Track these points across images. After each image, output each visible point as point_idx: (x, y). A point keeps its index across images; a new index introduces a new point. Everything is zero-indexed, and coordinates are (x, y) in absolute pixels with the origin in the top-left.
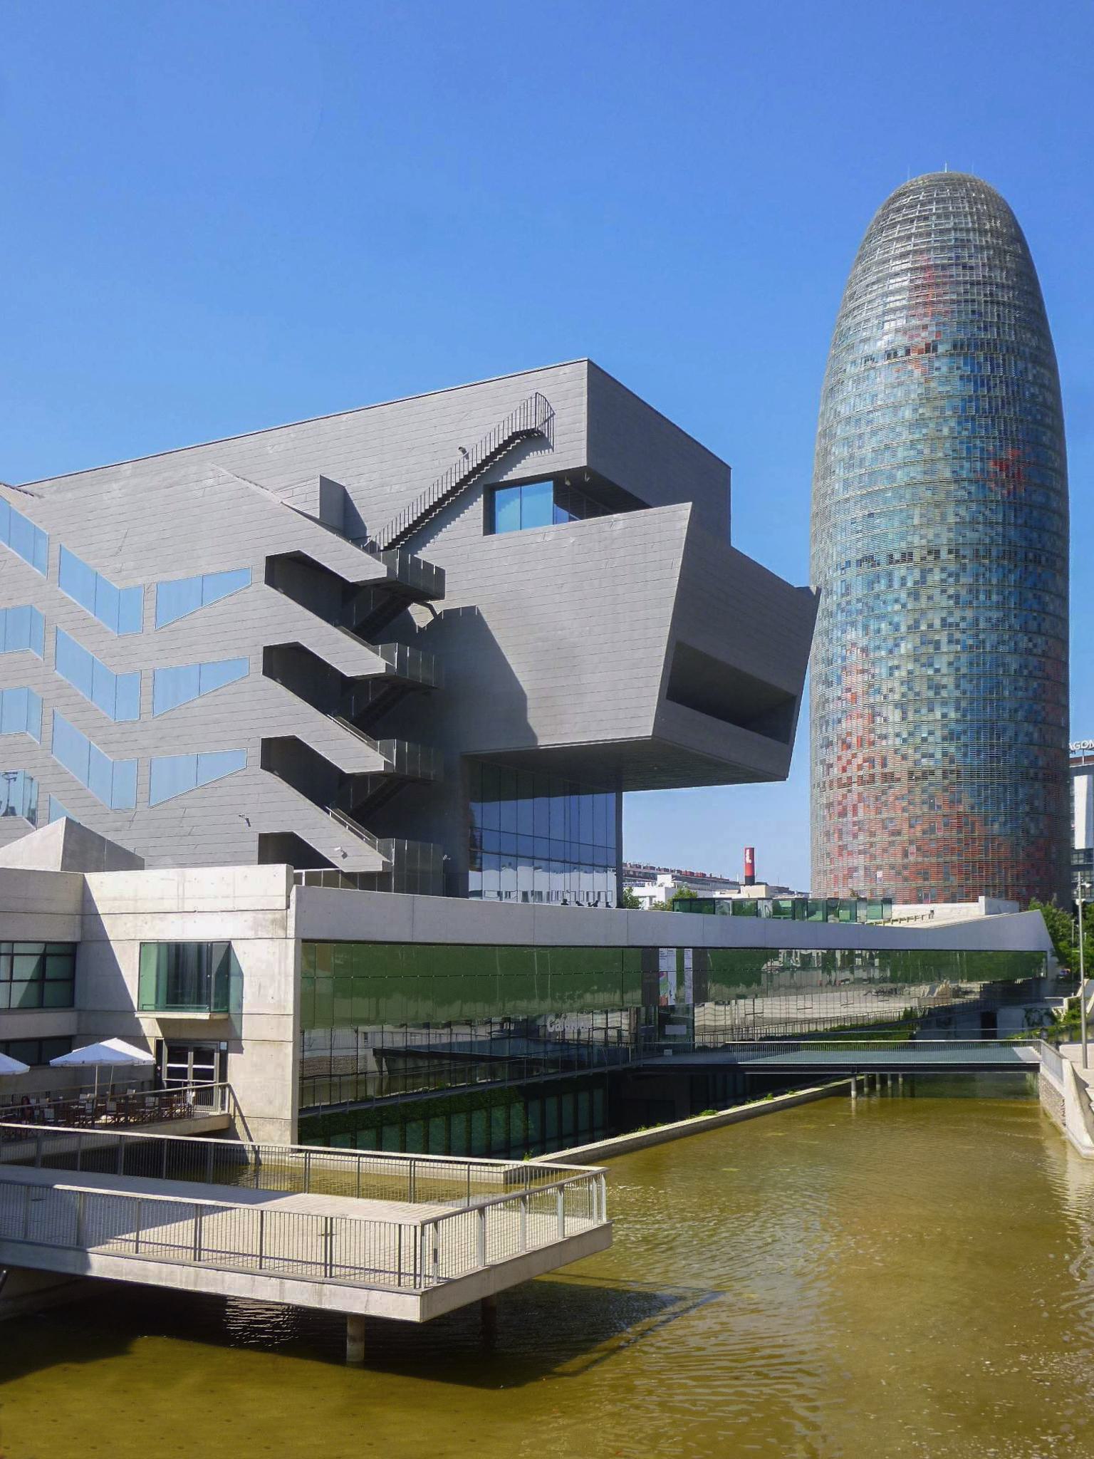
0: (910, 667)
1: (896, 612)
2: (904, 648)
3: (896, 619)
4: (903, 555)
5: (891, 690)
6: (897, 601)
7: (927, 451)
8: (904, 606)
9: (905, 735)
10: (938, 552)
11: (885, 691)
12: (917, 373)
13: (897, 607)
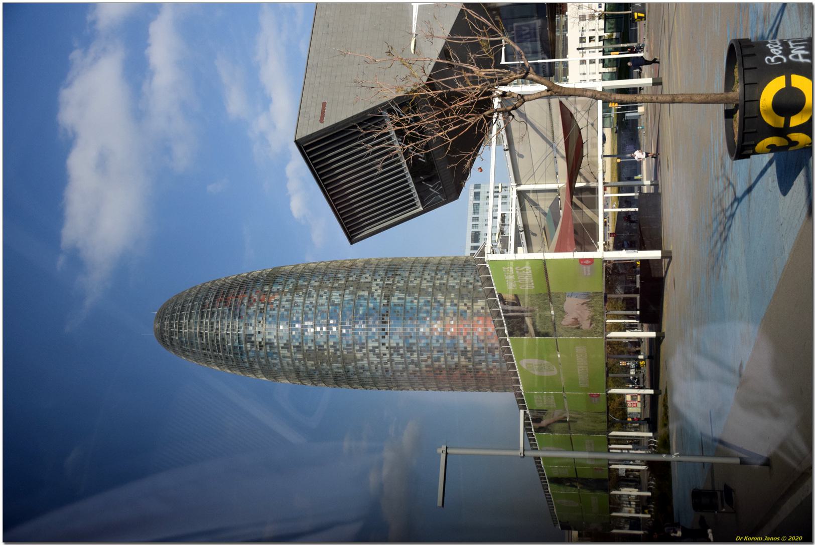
0: (453, 295)
1: (418, 302)
2: (440, 297)
3: (422, 301)
6: (412, 302)
7: (326, 290)
12: (277, 297)
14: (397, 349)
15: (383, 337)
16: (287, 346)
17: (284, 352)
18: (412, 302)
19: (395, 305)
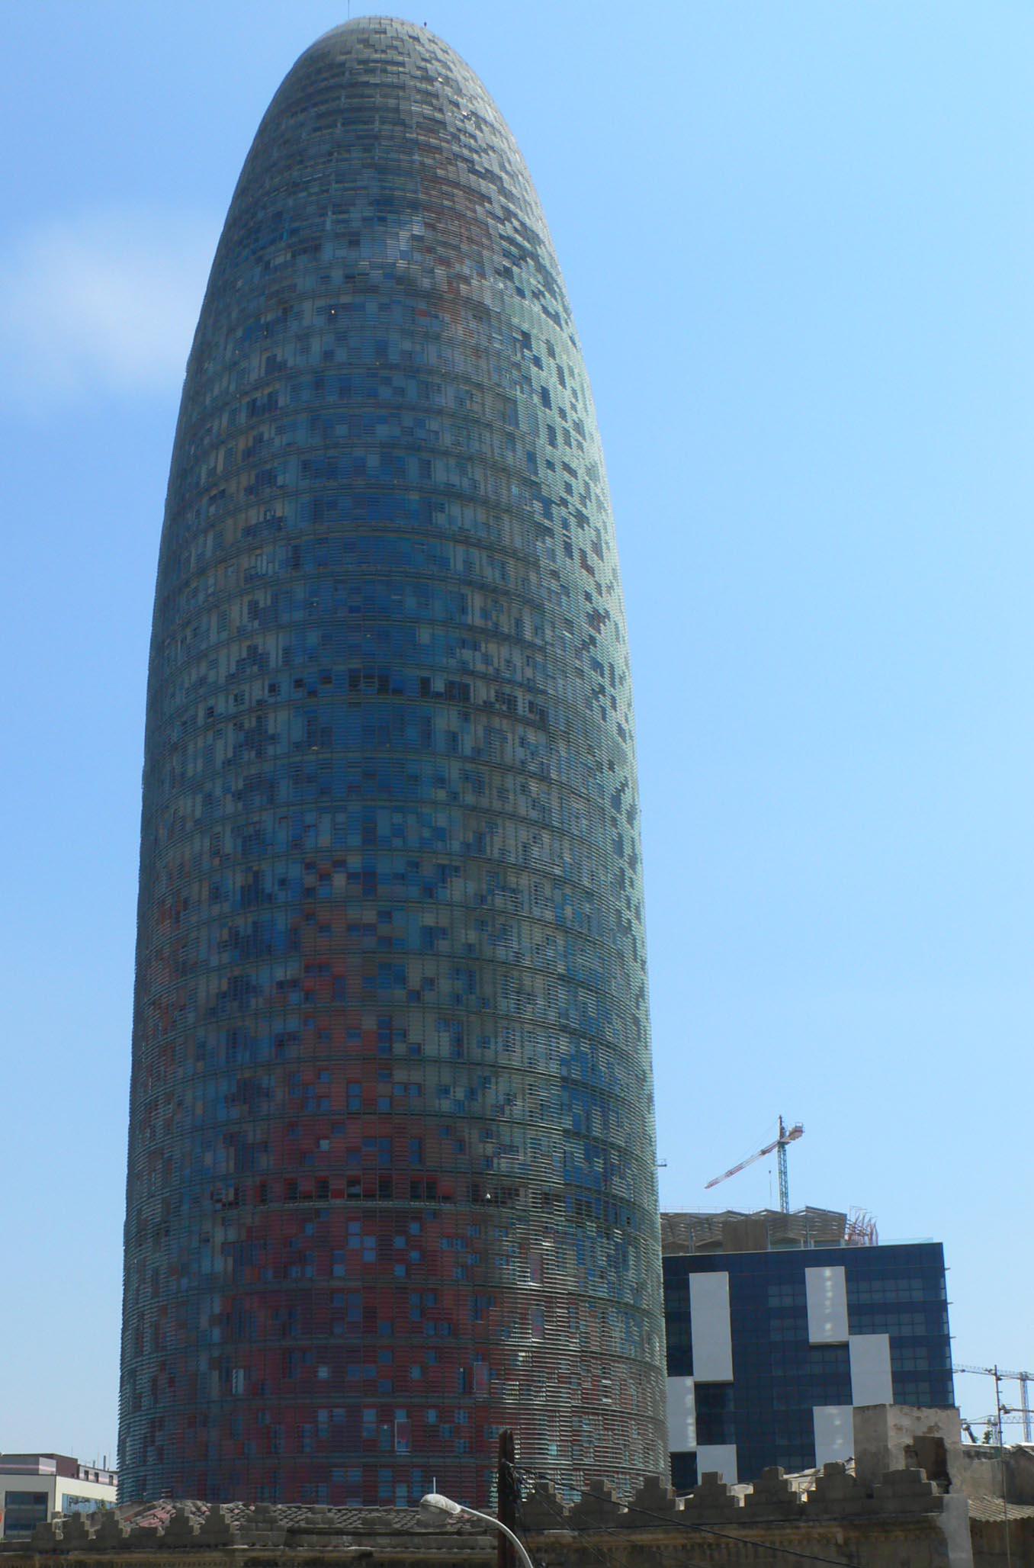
3: (441, 821)
4: (450, 685)
5: (430, 982)
6: (440, 781)
8: (454, 796)
9: (460, 1094)
10: (511, 702)
11: (414, 980)
13: (442, 795)
14: (256, 740)
15: (299, 683)
16: (274, 366)
17: (256, 366)
18: (440, 781)
19: (428, 721)
